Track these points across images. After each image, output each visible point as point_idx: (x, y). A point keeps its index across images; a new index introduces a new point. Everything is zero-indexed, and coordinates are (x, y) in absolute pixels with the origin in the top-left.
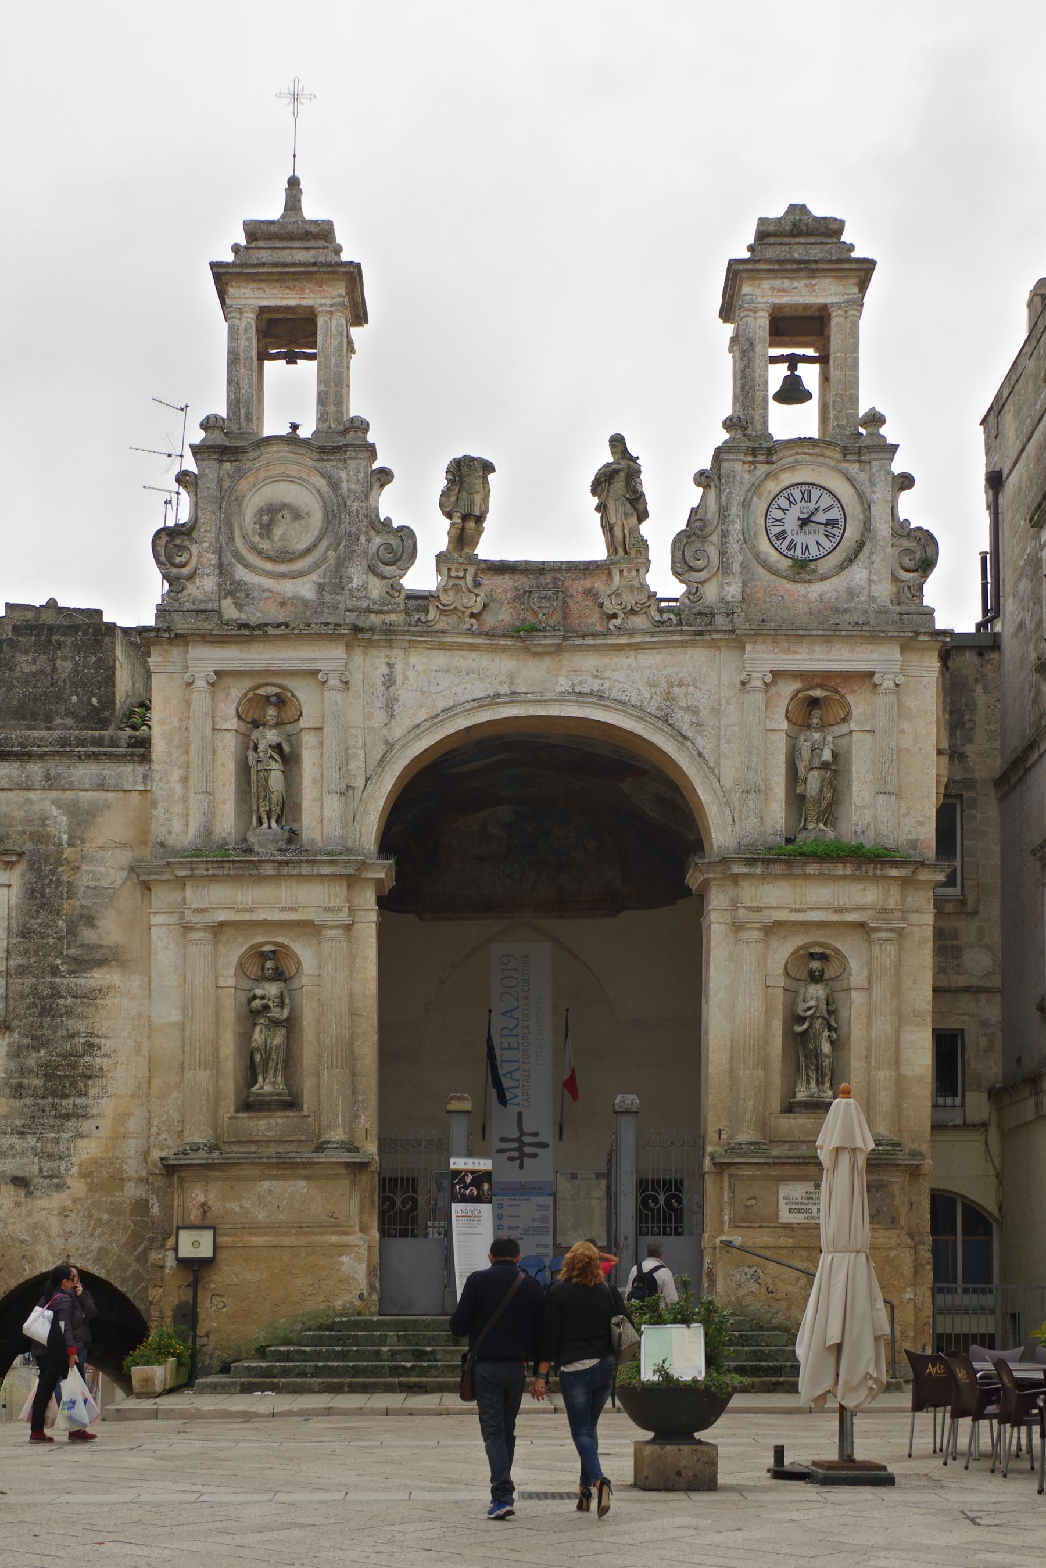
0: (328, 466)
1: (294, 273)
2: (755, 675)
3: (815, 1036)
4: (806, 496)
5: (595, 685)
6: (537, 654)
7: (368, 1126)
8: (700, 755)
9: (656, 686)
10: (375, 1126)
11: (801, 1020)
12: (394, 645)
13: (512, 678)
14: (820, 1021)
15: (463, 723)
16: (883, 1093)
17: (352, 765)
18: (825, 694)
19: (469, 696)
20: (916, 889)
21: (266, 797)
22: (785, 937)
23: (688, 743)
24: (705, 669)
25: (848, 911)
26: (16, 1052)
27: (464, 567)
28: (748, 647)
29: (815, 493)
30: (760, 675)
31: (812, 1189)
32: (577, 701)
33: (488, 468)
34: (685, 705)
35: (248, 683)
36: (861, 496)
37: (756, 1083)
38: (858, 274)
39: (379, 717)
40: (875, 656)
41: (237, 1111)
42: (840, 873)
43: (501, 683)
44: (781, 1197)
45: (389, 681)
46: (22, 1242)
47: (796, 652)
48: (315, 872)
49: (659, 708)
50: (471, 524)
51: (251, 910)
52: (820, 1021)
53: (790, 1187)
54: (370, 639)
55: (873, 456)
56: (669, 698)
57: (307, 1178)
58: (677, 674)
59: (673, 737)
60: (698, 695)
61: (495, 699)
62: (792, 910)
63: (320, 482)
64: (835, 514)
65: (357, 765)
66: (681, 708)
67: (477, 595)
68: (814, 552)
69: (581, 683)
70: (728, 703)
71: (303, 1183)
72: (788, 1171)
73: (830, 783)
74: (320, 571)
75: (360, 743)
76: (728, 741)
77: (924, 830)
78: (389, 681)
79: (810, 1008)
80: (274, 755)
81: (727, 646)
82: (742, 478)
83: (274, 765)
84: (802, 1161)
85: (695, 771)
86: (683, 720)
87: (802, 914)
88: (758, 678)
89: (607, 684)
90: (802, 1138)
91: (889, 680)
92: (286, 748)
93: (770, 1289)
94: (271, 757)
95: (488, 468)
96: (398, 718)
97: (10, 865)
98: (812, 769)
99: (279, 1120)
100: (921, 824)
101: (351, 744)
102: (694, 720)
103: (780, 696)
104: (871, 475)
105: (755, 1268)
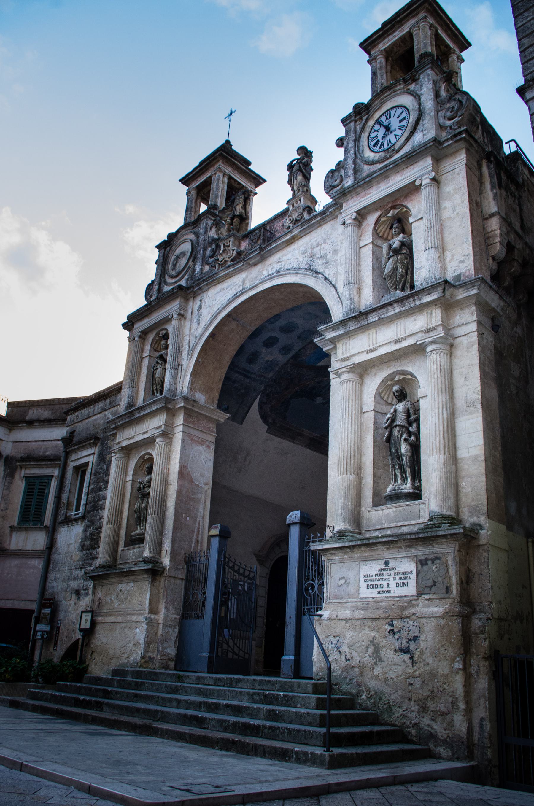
2: (346, 218)
3: (395, 442)
4: (388, 117)
7: (167, 549)
8: (326, 279)
10: (170, 548)
12: (203, 290)
14: (397, 429)
15: (224, 314)
16: (434, 475)
18: (396, 211)
20: (461, 309)
22: (375, 374)
23: (320, 276)
24: (330, 231)
25: (405, 339)
26: (85, 531)
27: (228, 240)
30: (349, 216)
31: (383, 567)
34: (319, 256)
35: (155, 333)
37: (346, 484)
40: (415, 170)
41: (125, 546)
44: (361, 575)
46: (74, 623)
47: (370, 194)
49: (307, 264)
51: (133, 438)
53: (368, 566)
54: (192, 291)
56: (312, 256)
57: (134, 581)
58: (316, 241)
61: (236, 297)
62: (368, 352)
66: (317, 258)
68: (393, 140)
69: (272, 269)
70: (342, 243)
71: (132, 584)
72: (365, 552)
74: (188, 273)
77: (465, 265)
83: (159, 366)
84: (367, 542)
86: (319, 265)
88: (349, 219)
90: (387, 526)
91: (425, 179)
93: (348, 657)
97: (95, 444)
99: (138, 550)
100: (462, 262)
105: (338, 638)
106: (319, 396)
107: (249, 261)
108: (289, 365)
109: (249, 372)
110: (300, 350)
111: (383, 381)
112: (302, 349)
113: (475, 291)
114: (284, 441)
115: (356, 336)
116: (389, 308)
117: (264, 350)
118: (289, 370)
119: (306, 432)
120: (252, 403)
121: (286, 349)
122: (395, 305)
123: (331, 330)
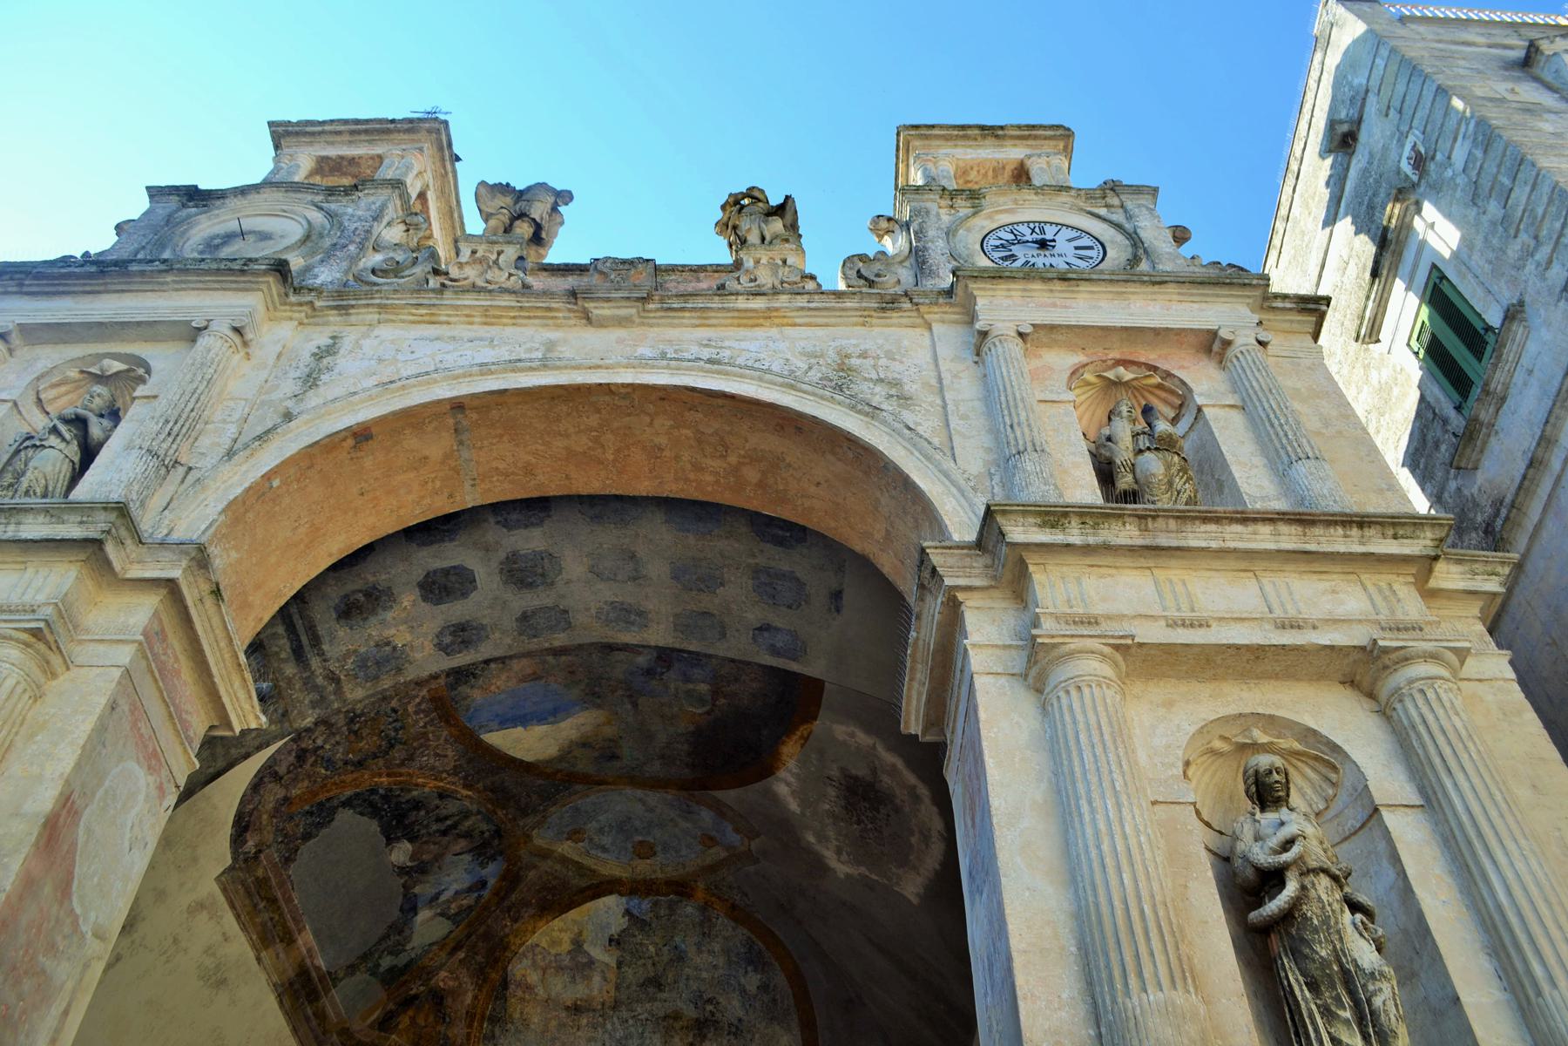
0: (333, 206)
1: (366, 132)
3: (1325, 921)
5: (706, 353)
6: (602, 324)
9: (822, 356)
11: (1272, 879)
12: (353, 319)
13: (550, 346)
15: (445, 391)
17: (205, 442)
19: (462, 362)
21: (11, 485)
22: (1169, 704)
24: (906, 343)
27: (497, 248)
28: (981, 303)
29: (1047, 227)
32: (668, 367)
33: (565, 197)
36: (1118, 226)
38: (1052, 143)
39: (289, 386)
42: (1272, 546)
43: (530, 350)
45: (325, 353)
48: (10, 535)
50: (524, 229)
52: (1324, 881)
55: (1123, 197)
59: (853, 408)
60: (896, 366)
61: (514, 365)
62: (1173, 624)
63: (317, 217)
64: (1086, 241)
65: (214, 440)
66: (866, 379)
67: (510, 275)
73: (1183, 470)
75: (237, 416)
76: (964, 417)
78: (325, 353)
79: (1288, 844)
80: (63, 428)
81: (943, 322)
82: (938, 215)
83: (53, 440)
85: (903, 452)
87: (1201, 632)
89: (727, 353)
92: (95, 431)
94: (54, 430)
95: (565, 197)
96: (321, 390)
98: (1141, 451)
101: (218, 416)
102: (893, 392)
103: (1051, 369)
104: (1126, 211)
106: (411, 840)
107: (589, 305)
108: (424, 692)
109: (316, 641)
110: (487, 662)
111: (1200, 731)
112: (495, 660)
113: (1493, 585)
114: (242, 938)
115: (1113, 571)
116: (1265, 529)
117: (409, 599)
118: (411, 709)
119: (306, 939)
120: (247, 756)
121: (461, 634)
122: (1283, 528)
123: (1039, 520)
